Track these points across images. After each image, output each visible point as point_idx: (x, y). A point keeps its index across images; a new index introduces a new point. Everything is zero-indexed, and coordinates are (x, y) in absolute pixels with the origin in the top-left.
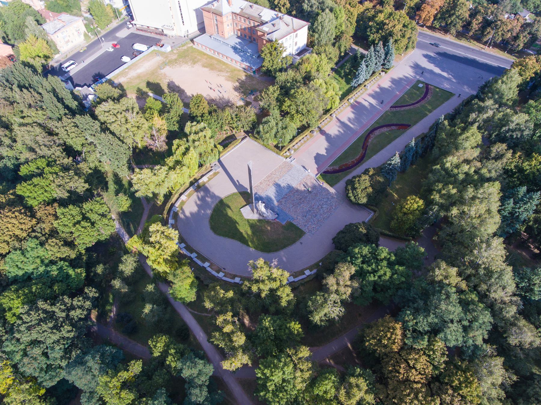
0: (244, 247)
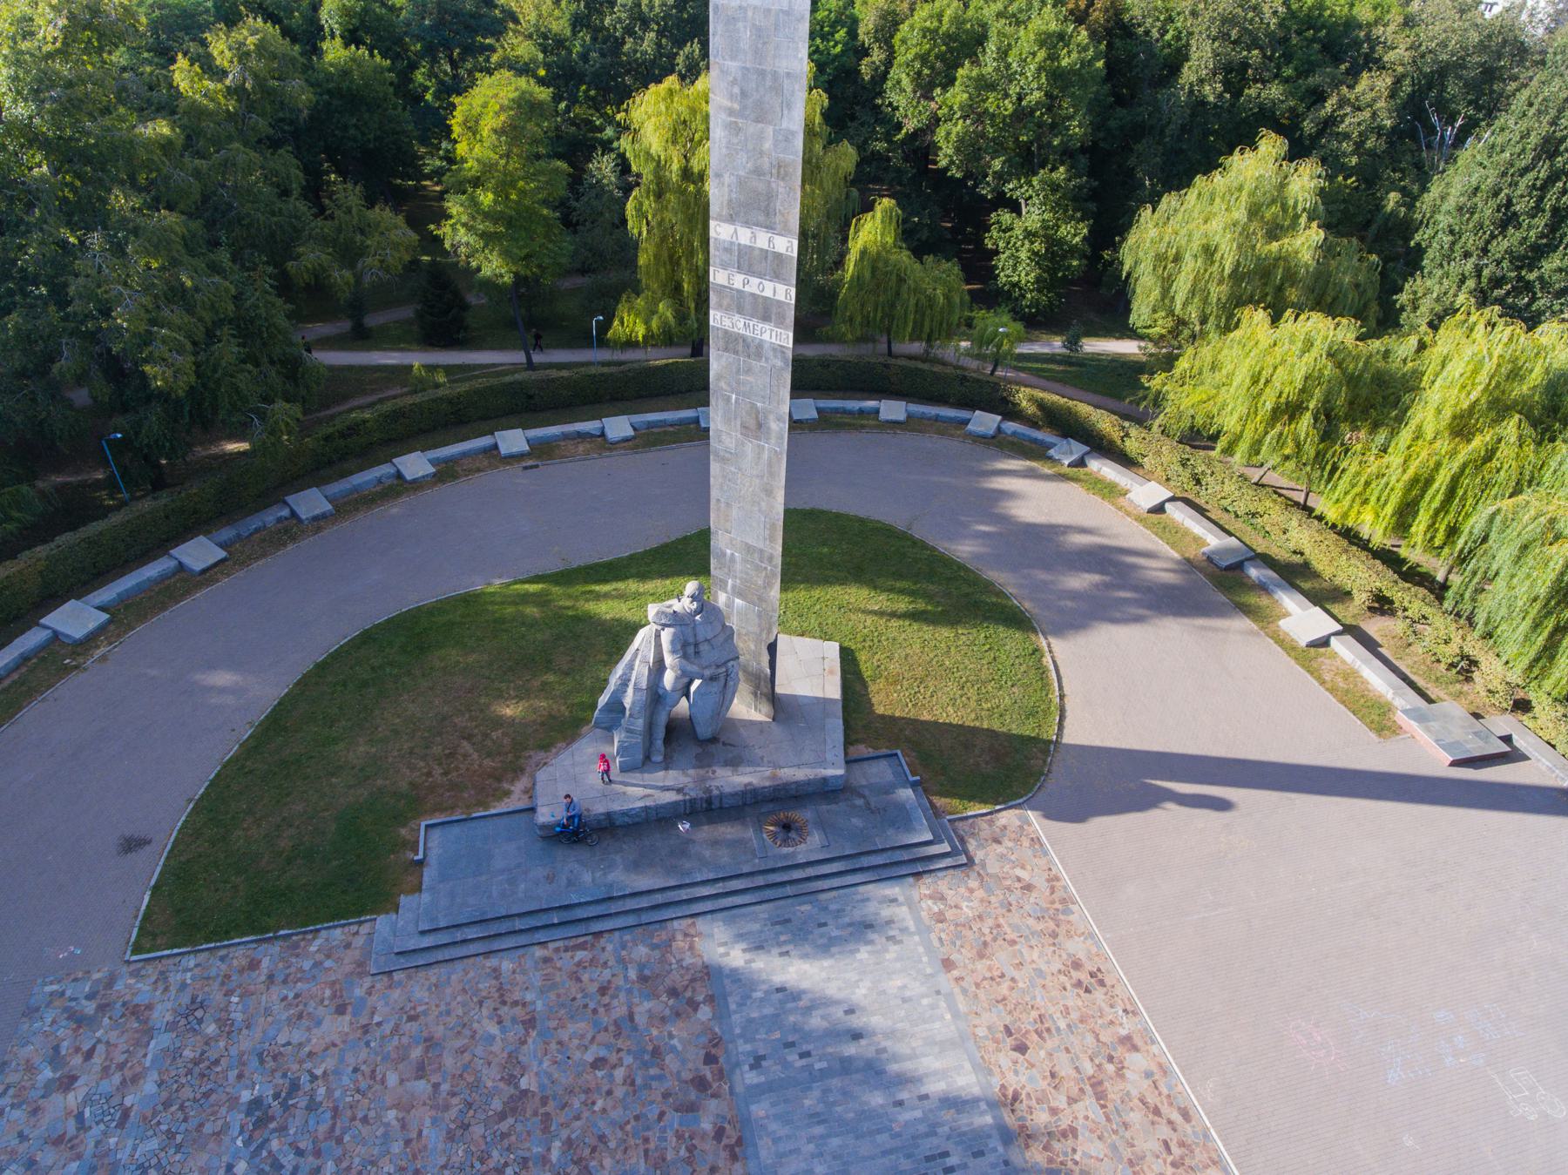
0: (553, 565)
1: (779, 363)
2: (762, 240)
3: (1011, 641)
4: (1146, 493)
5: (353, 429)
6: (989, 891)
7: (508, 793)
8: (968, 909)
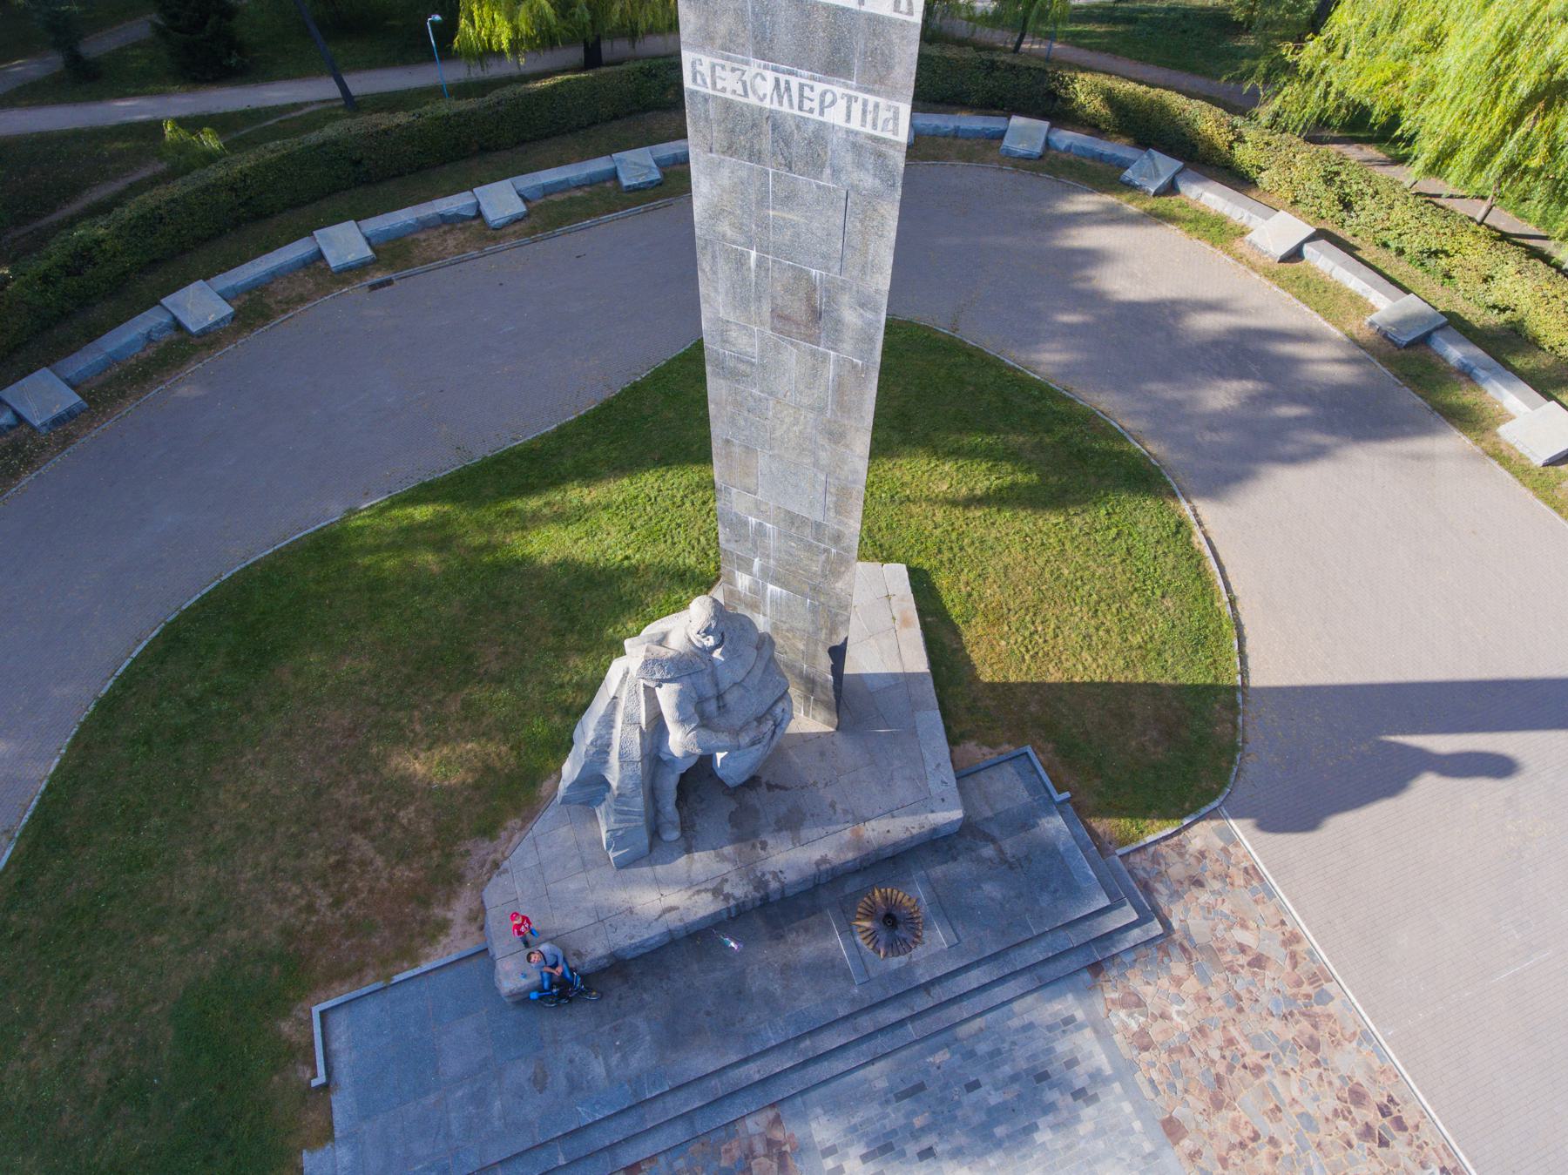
0: (445, 463)
1: (868, 181)
3: (1144, 514)
4: (1276, 231)
5: (84, 256)
6: (1204, 978)
7: (443, 926)
8: (1182, 1018)
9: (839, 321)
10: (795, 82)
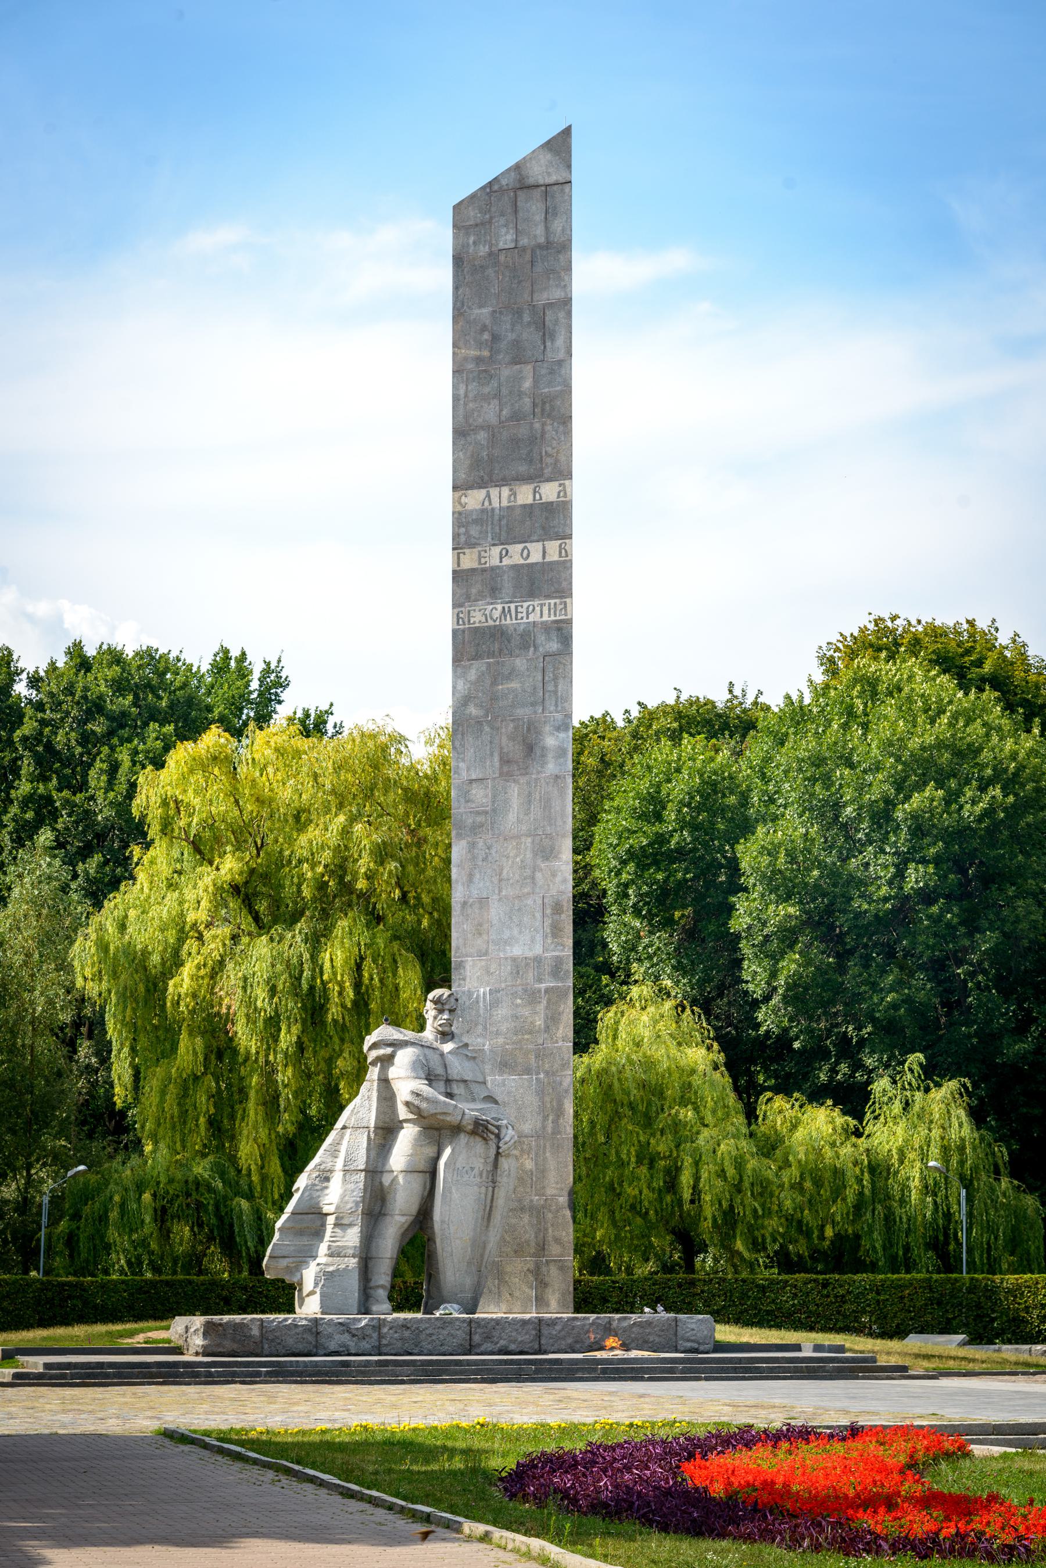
2: (525, 495)
9: (543, 748)
10: (513, 606)
